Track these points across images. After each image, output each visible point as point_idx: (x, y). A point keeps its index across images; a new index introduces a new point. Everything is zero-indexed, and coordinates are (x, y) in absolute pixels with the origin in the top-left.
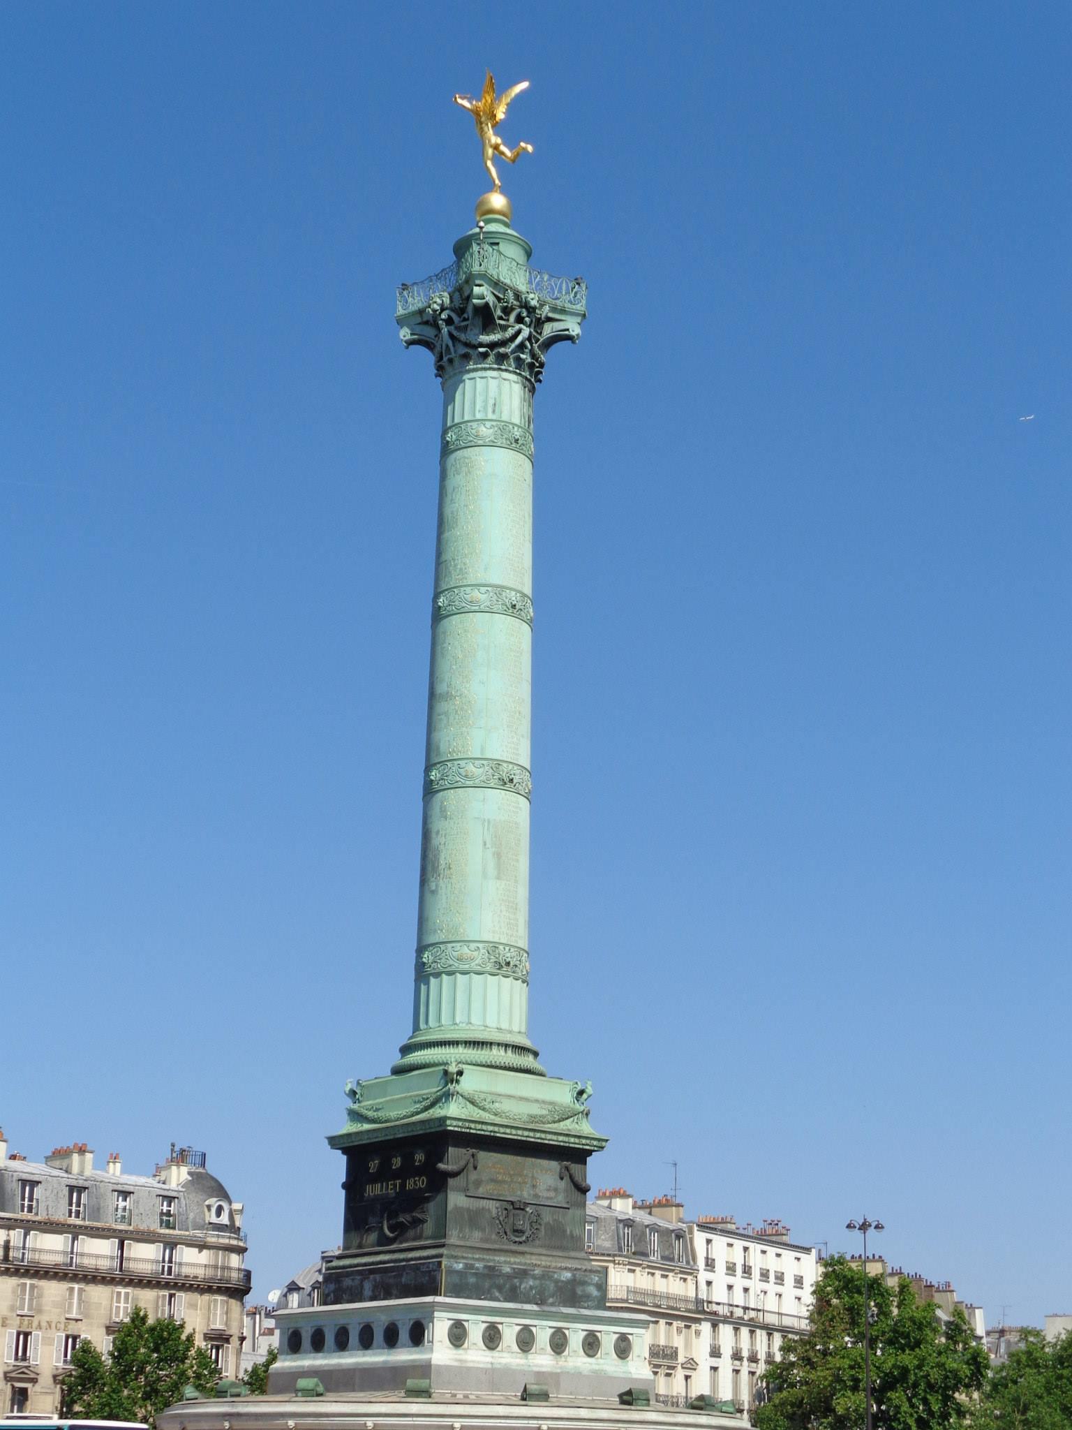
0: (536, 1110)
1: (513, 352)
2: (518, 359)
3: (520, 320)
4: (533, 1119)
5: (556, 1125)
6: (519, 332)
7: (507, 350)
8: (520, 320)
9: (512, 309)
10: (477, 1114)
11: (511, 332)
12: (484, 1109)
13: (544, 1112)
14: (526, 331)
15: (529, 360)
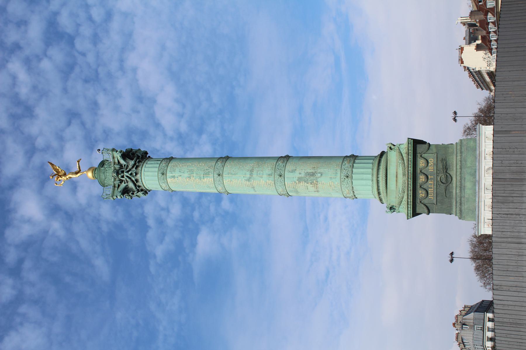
0: (400, 172)
1: (133, 176)
2: (136, 174)
3: (123, 177)
4: (404, 175)
5: (405, 161)
6: (127, 176)
7: (134, 179)
8: (123, 177)
9: (120, 180)
10: (404, 202)
11: (128, 179)
12: (403, 197)
13: (401, 166)
14: (125, 174)
15: (134, 169)
